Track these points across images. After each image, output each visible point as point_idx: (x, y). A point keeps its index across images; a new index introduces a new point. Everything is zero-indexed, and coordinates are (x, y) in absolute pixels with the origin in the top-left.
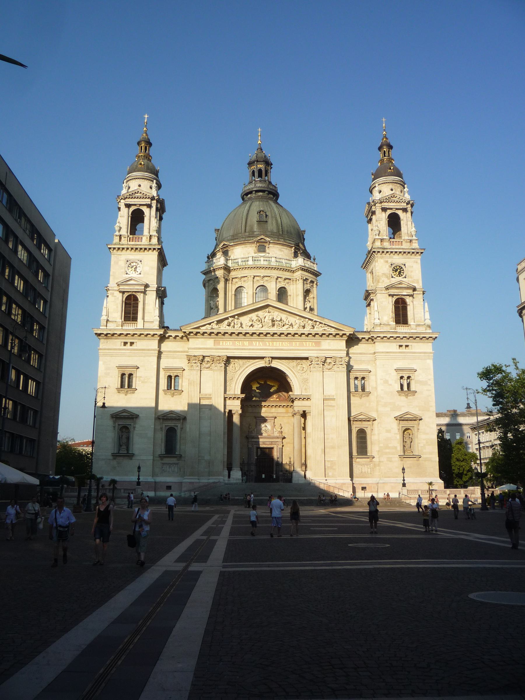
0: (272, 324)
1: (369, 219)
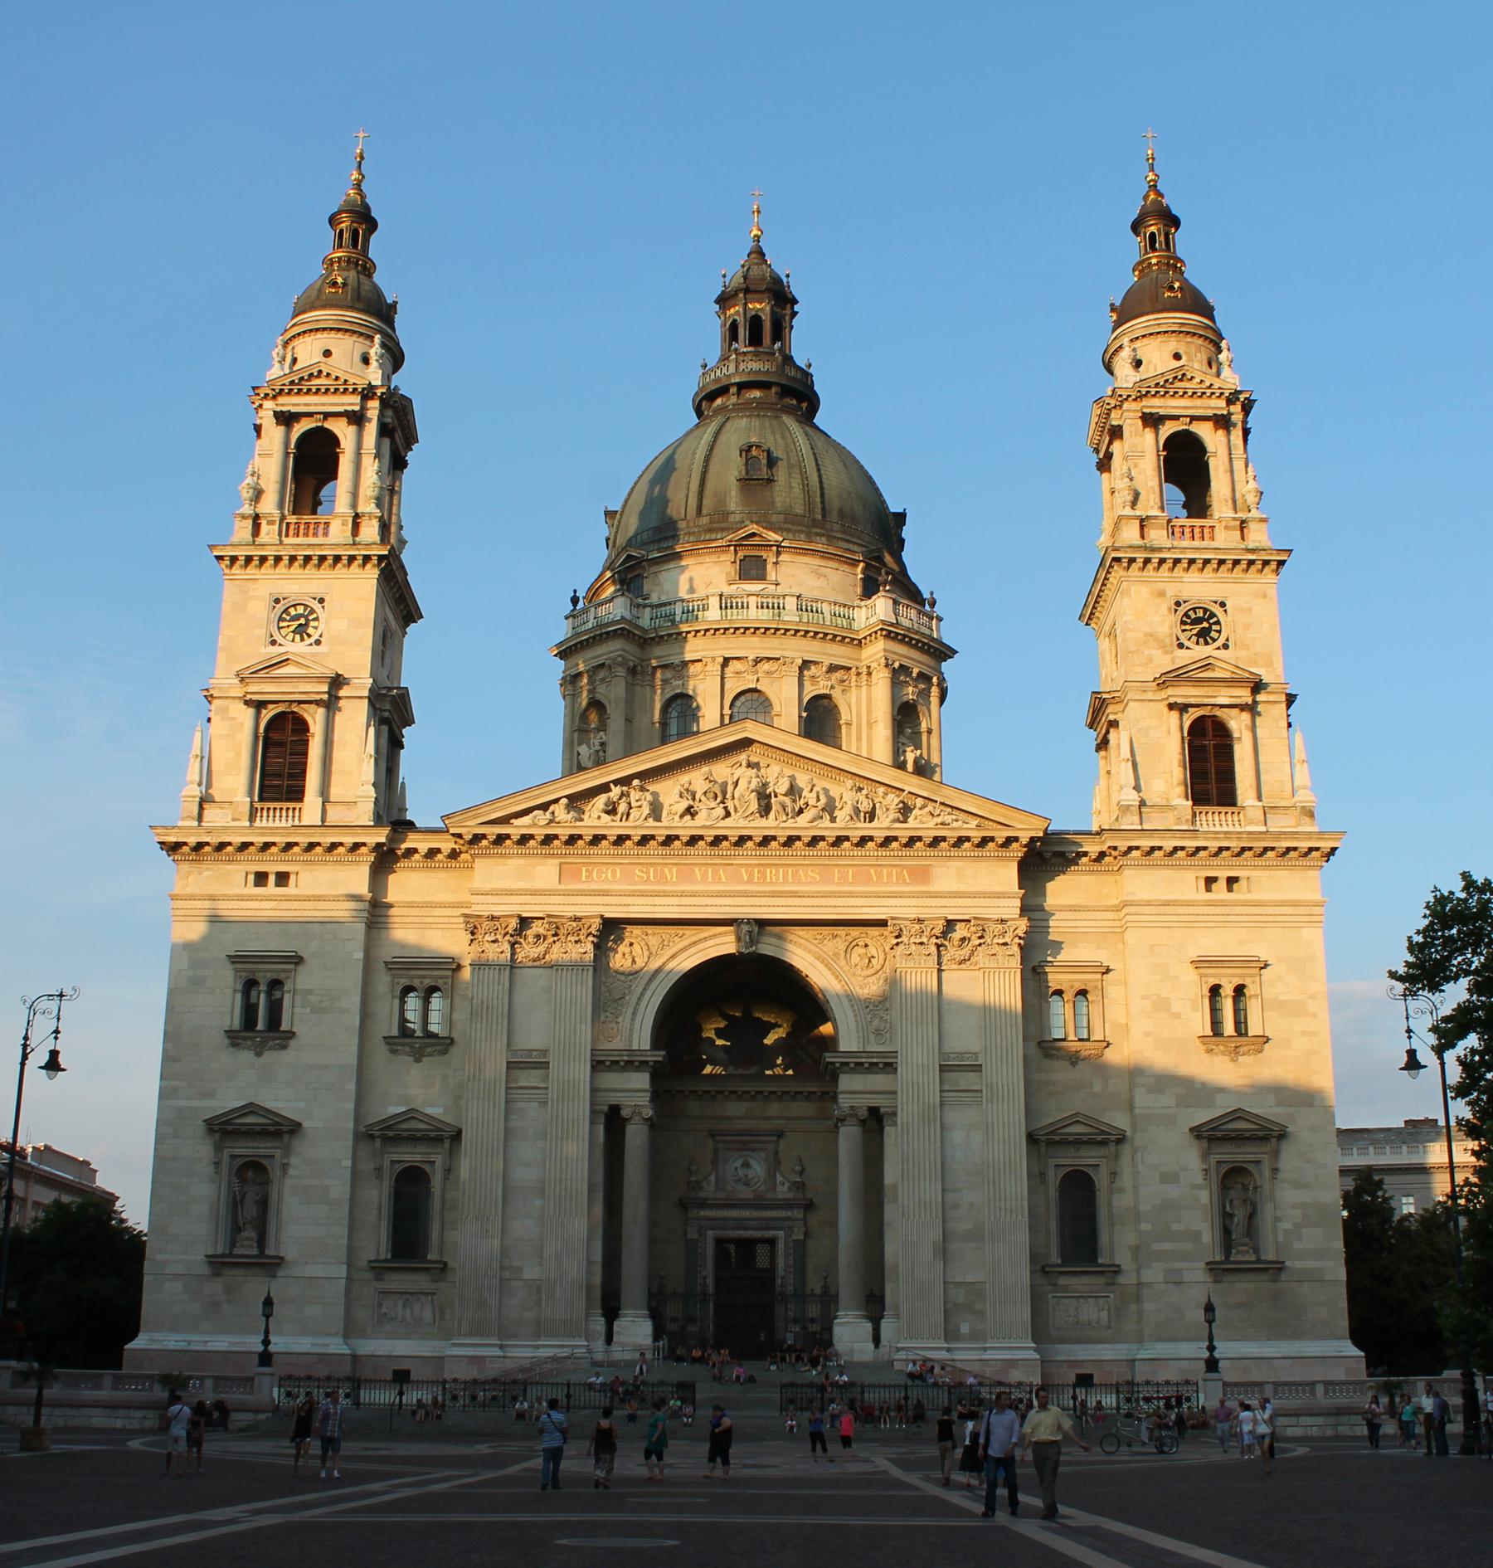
0: (759, 805)
1: (1101, 456)
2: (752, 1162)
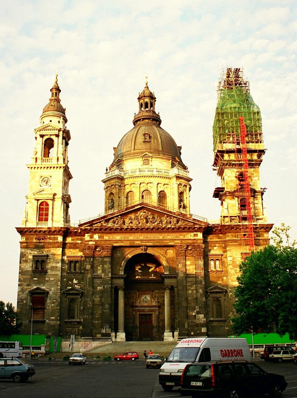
2: (147, 297)
